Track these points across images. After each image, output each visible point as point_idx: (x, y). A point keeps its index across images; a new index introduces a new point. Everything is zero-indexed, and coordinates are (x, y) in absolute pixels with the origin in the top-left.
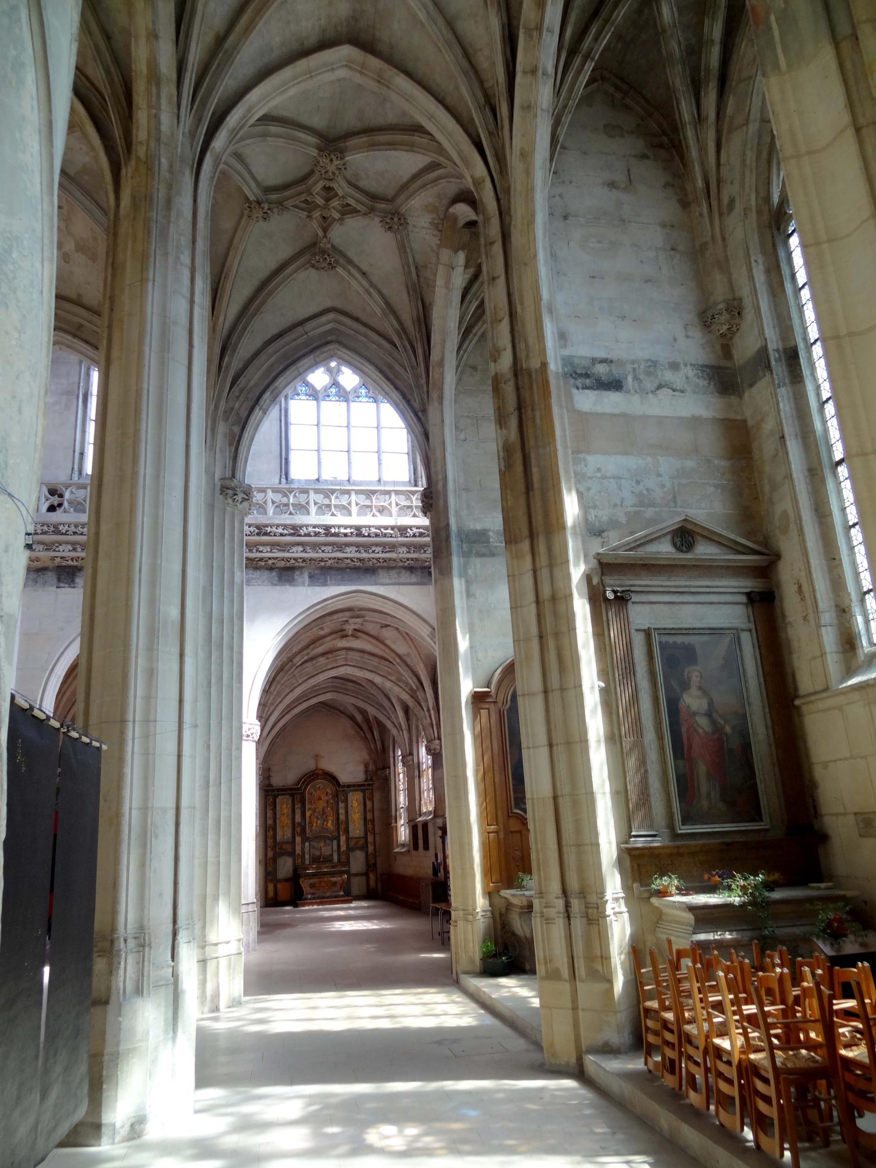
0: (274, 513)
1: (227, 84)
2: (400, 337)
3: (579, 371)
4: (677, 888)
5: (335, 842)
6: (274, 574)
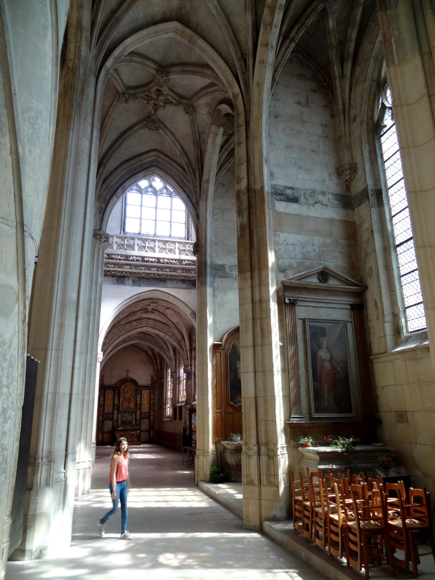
0: (116, 248)
1: (116, 34)
2: (188, 167)
3: (278, 192)
4: (312, 443)
5: (134, 414)
6: (115, 279)
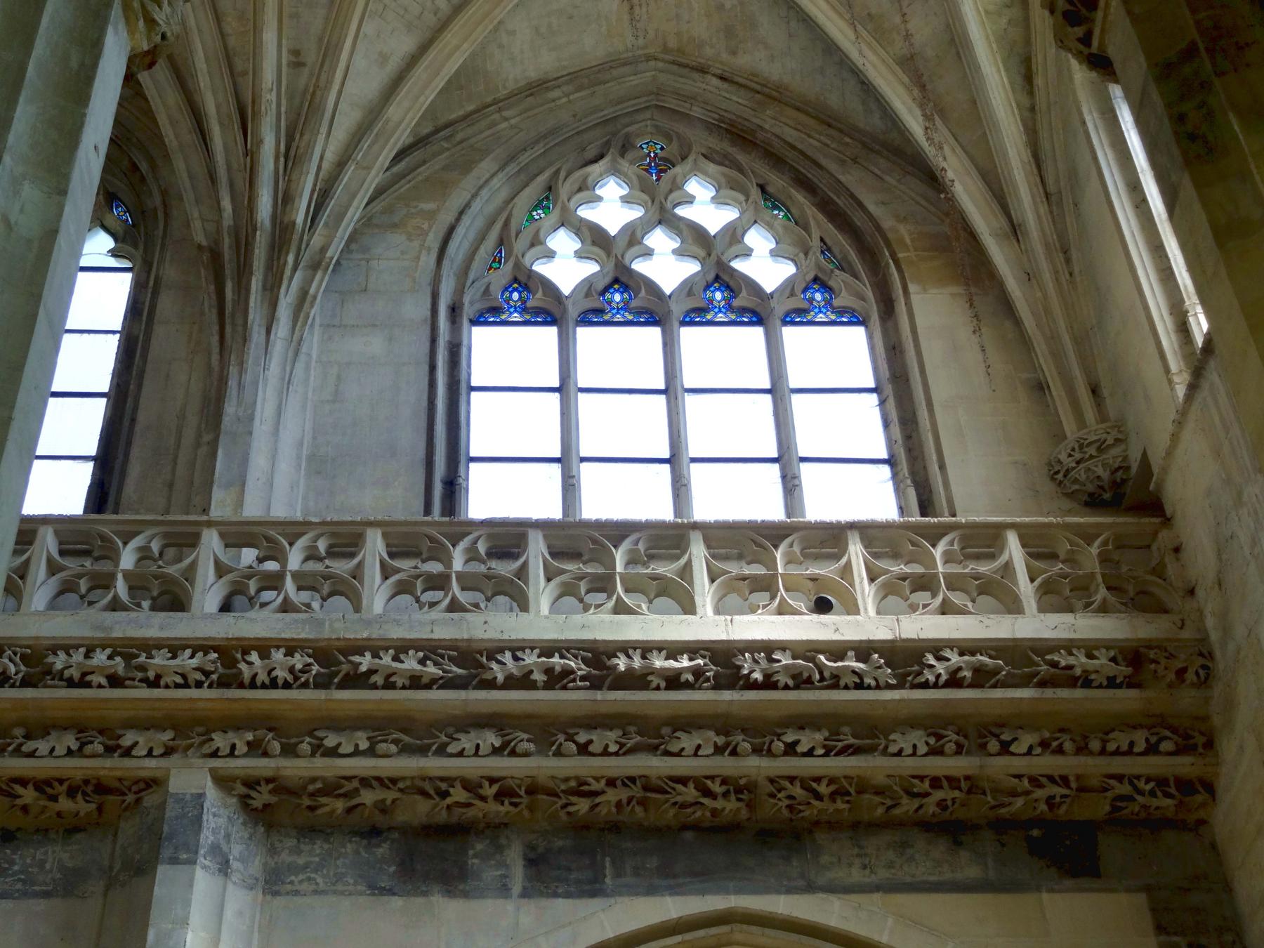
6: (383, 850)
